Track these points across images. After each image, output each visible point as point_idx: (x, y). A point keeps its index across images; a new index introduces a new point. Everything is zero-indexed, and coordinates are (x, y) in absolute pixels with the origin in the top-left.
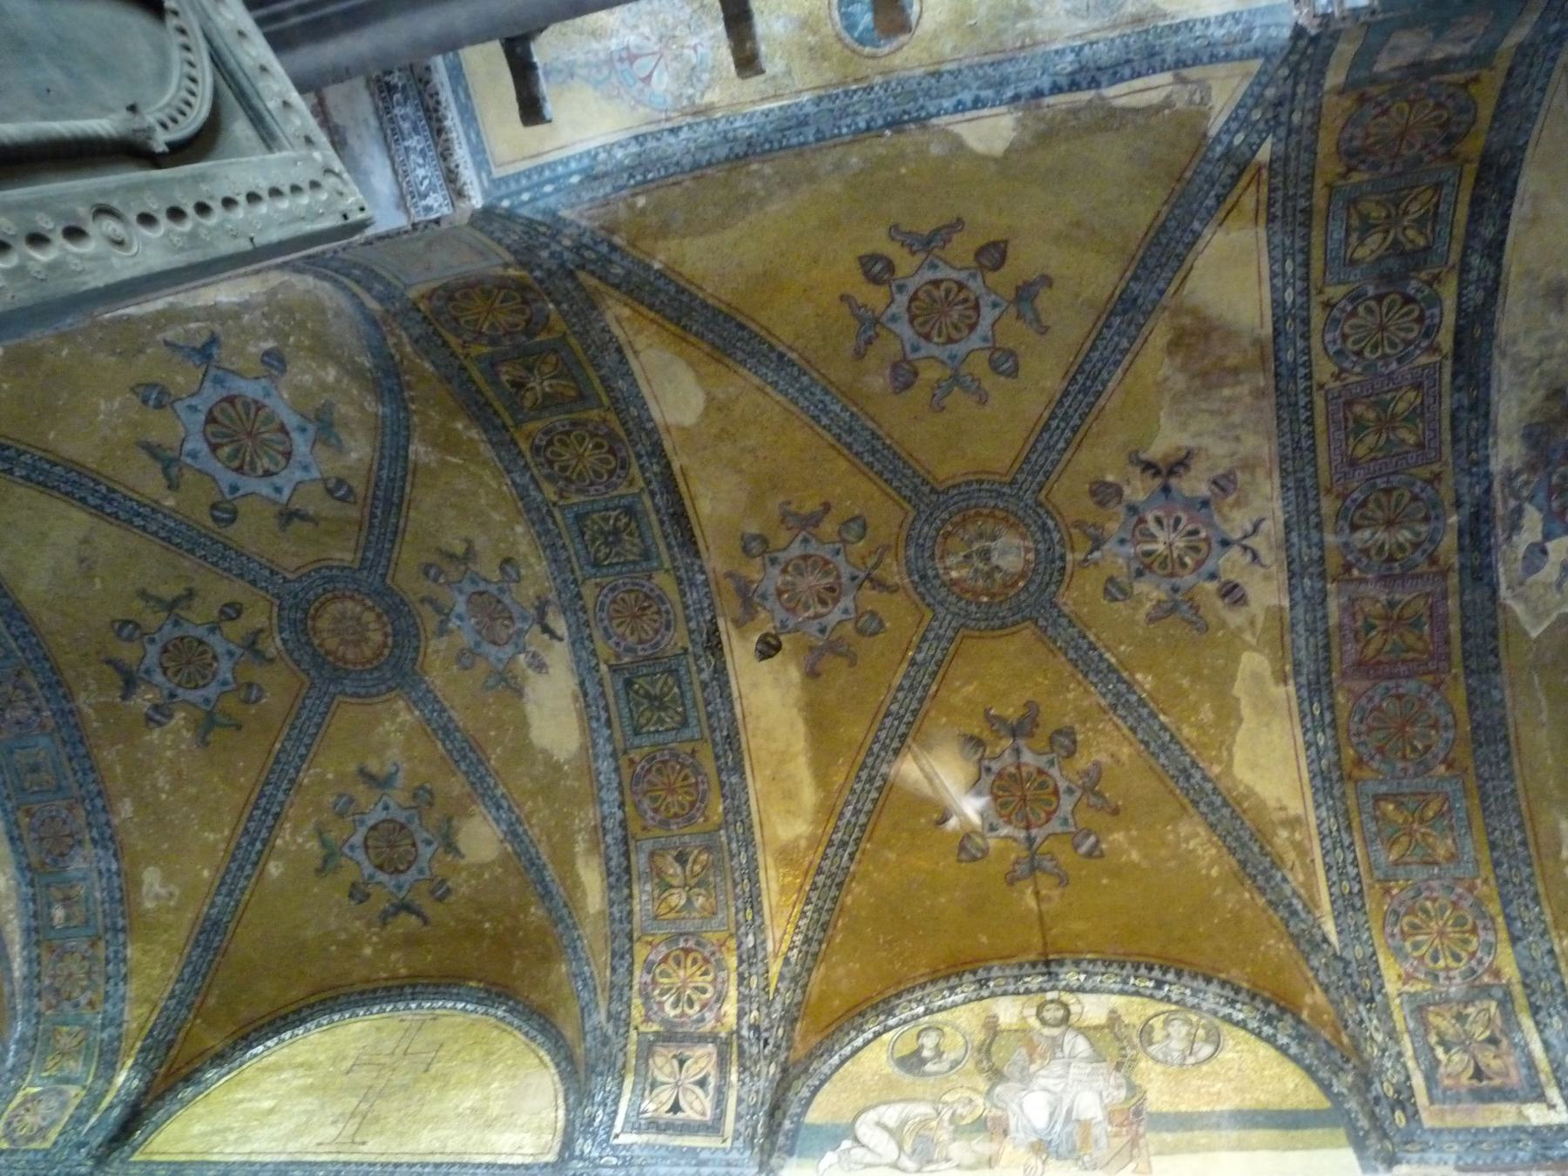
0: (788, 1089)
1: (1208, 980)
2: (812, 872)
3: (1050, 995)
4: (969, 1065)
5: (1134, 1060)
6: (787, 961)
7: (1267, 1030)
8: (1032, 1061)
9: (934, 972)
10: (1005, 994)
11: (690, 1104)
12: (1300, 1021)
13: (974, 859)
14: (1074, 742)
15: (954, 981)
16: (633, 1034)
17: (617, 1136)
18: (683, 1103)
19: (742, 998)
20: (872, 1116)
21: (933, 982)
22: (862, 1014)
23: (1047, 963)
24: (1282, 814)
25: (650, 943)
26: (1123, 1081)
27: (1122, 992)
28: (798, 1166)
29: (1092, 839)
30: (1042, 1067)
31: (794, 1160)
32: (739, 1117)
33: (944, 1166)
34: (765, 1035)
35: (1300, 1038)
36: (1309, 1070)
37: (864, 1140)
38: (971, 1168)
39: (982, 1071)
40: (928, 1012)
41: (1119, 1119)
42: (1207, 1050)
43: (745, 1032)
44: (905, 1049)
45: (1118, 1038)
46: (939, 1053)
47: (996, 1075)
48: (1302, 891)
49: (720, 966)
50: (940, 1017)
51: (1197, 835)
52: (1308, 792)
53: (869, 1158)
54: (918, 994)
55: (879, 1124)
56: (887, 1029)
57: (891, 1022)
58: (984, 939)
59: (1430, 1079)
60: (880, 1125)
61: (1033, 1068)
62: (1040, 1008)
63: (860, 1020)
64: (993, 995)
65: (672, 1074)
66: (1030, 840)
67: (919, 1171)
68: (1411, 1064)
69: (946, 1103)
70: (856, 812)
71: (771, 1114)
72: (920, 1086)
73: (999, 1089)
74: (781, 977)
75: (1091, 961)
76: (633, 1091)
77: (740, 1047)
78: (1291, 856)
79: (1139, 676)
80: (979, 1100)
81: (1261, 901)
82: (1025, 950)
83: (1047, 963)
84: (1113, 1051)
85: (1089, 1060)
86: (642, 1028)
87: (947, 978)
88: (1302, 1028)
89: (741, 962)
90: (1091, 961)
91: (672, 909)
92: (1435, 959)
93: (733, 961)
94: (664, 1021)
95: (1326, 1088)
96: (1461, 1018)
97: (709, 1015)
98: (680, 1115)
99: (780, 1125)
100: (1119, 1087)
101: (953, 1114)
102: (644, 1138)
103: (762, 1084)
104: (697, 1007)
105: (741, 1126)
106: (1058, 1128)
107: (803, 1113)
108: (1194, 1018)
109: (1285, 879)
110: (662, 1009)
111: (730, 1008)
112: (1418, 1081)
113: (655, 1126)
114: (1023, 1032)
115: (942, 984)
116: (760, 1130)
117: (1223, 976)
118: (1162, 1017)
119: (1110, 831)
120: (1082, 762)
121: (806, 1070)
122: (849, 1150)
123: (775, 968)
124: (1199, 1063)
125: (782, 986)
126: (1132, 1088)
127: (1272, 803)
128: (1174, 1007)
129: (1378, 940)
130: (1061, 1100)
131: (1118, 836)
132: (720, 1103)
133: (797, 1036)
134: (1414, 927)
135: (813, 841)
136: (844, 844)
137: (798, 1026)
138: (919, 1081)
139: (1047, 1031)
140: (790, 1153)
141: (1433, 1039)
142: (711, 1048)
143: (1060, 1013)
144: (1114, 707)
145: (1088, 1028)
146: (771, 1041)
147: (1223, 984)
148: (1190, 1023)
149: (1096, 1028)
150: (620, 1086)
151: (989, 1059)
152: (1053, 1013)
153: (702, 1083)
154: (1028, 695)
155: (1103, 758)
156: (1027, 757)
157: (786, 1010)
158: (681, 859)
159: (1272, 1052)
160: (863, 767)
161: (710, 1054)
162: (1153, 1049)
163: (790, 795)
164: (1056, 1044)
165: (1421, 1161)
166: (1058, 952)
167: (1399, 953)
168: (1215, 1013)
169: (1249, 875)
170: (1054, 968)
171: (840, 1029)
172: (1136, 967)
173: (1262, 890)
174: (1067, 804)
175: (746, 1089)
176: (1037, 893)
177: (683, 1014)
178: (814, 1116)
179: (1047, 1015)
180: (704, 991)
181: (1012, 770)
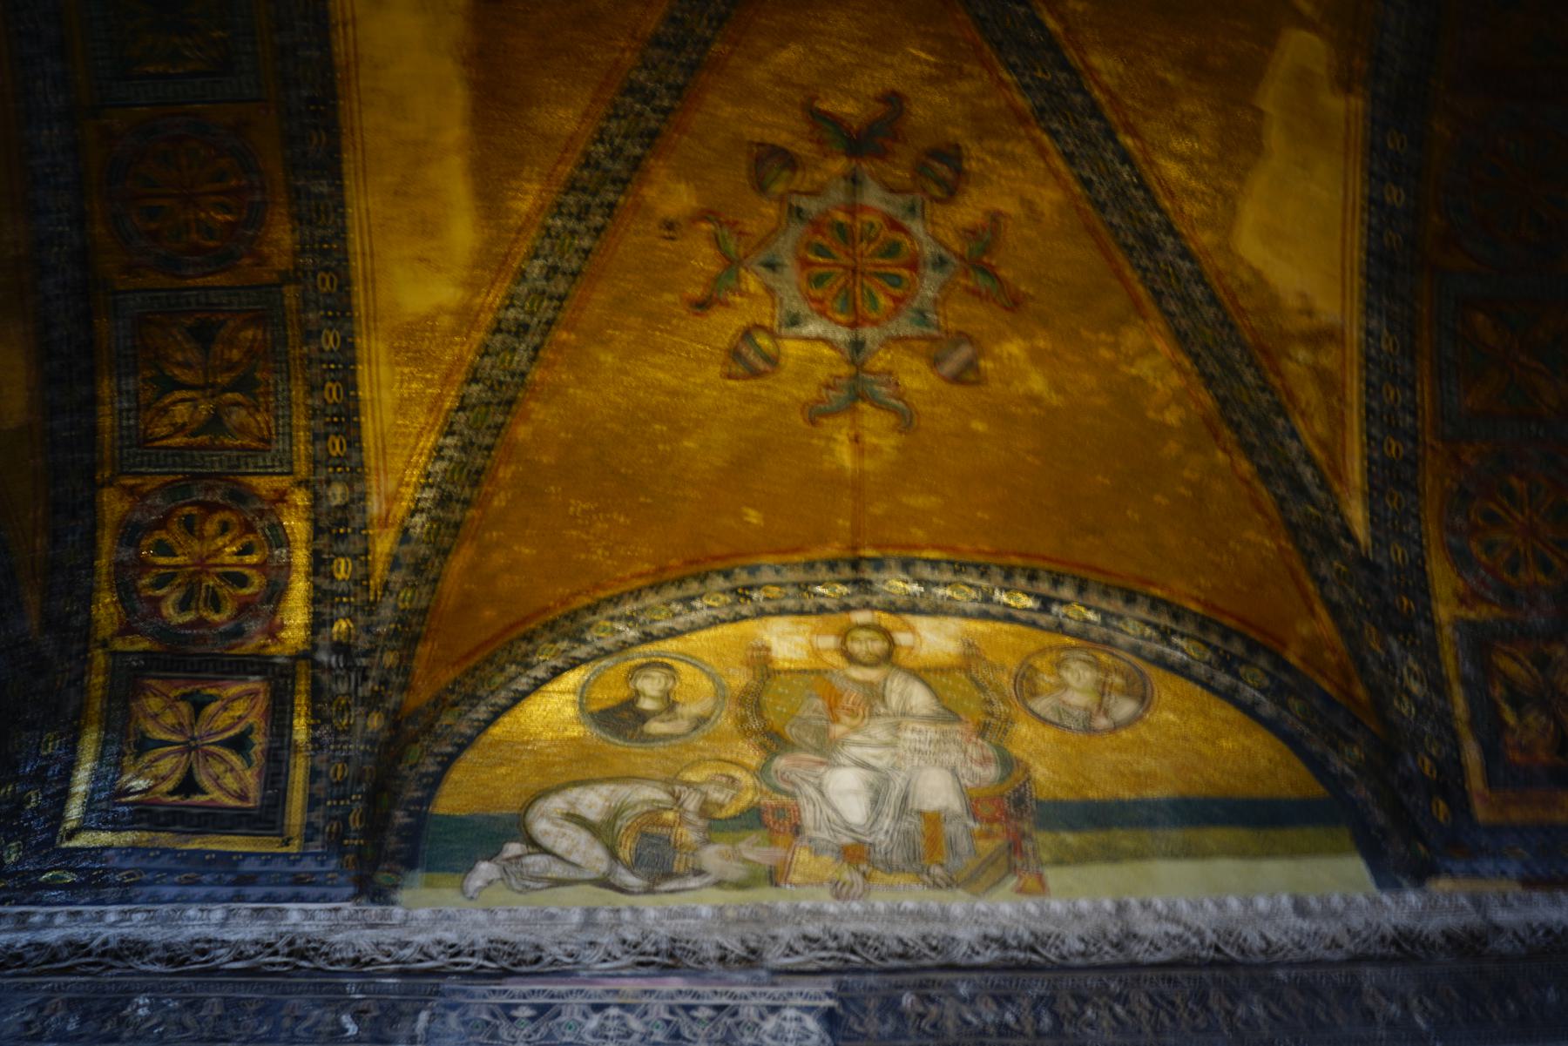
0: (399, 758)
1: (1130, 598)
2: (460, 377)
3: (861, 617)
4: (726, 722)
5: (1009, 721)
6: (405, 536)
7: (1224, 679)
8: (836, 720)
9: (662, 569)
10: (782, 612)
11: (216, 779)
12: (1281, 664)
13: (755, 374)
14: (959, 172)
15: (693, 587)
16: (100, 659)
17: (71, 834)
18: (204, 780)
19: (318, 598)
20: (557, 803)
21: (656, 587)
22: (529, 638)
23: (855, 564)
24: (1304, 323)
25: (131, 490)
26: (991, 753)
27: (984, 616)
28: (429, 885)
29: (965, 352)
30: (855, 730)
31: (419, 876)
32: (313, 802)
33: (693, 882)
34: (364, 662)
35: (1278, 693)
36: (1292, 741)
37: (547, 842)
38: (740, 885)
39: (746, 733)
40: (648, 638)
41: (986, 810)
42: (1125, 708)
43: (323, 657)
44: (609, 694)
45: (980, 687)
46: (669, 705)
47: (774, 742)
48: (1317, 453)
49: (280, 539)
50: (671, 645)
51: (1153, 349)
52: (1358, 281)
53: (558, 871)
54: (628, 608)
55: (574, 818)
56: (574, 664)
57: (582, 652)
58: (753, 517)
59: (1491, 753)
60: (574, 818)
61: (838, 730)
62: (845, 634)
63: (524, 647)
64: (761, 613)
65: (178, 728)
66: (857, 346)
67: (649, 891)
68: (1464, 730)
69: (689, 784)
70: (551, 272)
71: (371, 799)
72: (636, 756)
73: (781, 763)
74: (395, 563)
75: (934, 564)
76: (100, 757)
77: (315, 681)
78: (1309, 394)
79: (1096, 60)
80: (745, 779)
81: (1245, 466)
82: (822, 540)
83: (855, 564)
84: (972, 706)
85: (932, 719)
86: (119, 645)
87: (680, 582)
88: (1285, 678)
89: (317, 531)
90: (934, 564)
91: (179, 429)
92: (1514, 570)
93: (297, 526)
94: (165, 633)
95: (1317, 766)
96: (1543, 662)
97: (254, 626)
98: (199, 799)
99: (388, 817)
100: (984, 761)
101: (705, 802)
102: (128, 837)
103: (356, 747)
104: (228, 610)
105: (317, 817)
106: (887, 823)
107: (429, 799)
108: (1103, 657)
109: (1294, 434)
110: (157, 612)
111: (296, 616)
112: (1472, 754)
113: (147, 815)
114: (814, 675)
115: (673, 592)
116: (355, 824)
117: (1158, 592)
118: (1052, 656)
119: (1000, 337)
120: (969, 211)
121: (429, 729)
122: (519, 857)
123: (384, 545)
124: (1116, 727)
125: (397, 577)
126: (1008, 763)
127: (1292, 302)
128: (1067, 640)
129: (1432, 530)
130: (887, 780)
131: (1014, 348)
132: (275, 777)
133: (419, 667)
134: (1491, 517)
135: (466, 316)
136: (522, 329)
137: (423, 650)
138: (637, 749)
139: (857, 673)
140: (411, 863)
141: (1498, 692)
142: (255, 683)
143: (878, 646)
144: (1040, 113)
145: (927, 670)
146: (373, 673)
147: (1155, 604)
148: (1096, 665)
149: (942, 670)
150: (72, 748)
151: (760, 715)
152: (866, 645)
153: (239, 744)
154: (889, 80)
155: (1009, 206)
156: (873, 196)
157: (402, 619)
158: (203, 335)
159: (1232, 713)
160: (572, 186)
161: (253, 694)
162: (1041, 705)
163: (428, 228)
164: (875, 694)
165: (1475, 874)
166: (877, 546)
167: (1460, 560)
168: (1136, 651)
169: (1230, 422)
170: (869, 574)
171: (489, 661)
172: (1009, 573)
173: (1249, 450)
174: (929, 287)
175: (325, 755)
176: (856, 439)
177: (201, 622)
178: (451, 801)
179: (856, 648)
180: (242, 581)
181: (841, 217)
